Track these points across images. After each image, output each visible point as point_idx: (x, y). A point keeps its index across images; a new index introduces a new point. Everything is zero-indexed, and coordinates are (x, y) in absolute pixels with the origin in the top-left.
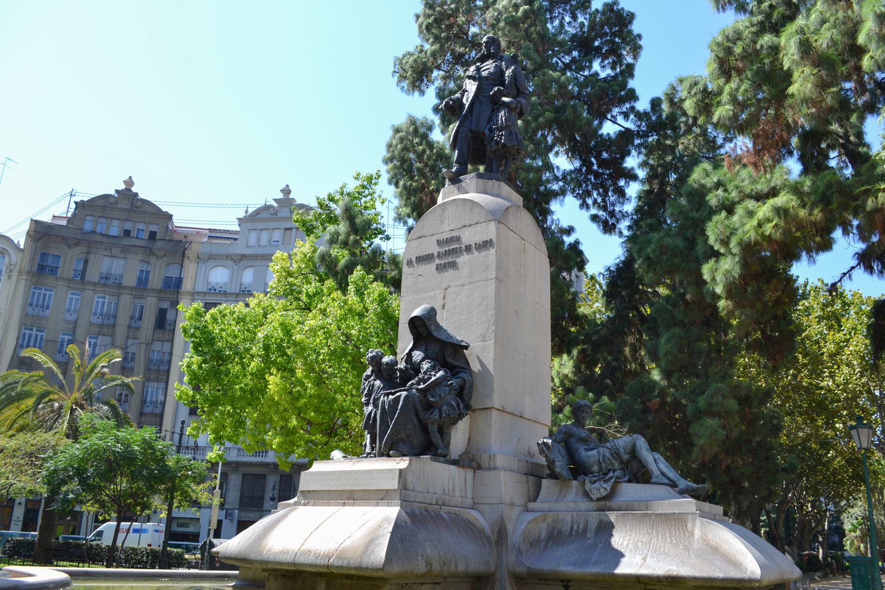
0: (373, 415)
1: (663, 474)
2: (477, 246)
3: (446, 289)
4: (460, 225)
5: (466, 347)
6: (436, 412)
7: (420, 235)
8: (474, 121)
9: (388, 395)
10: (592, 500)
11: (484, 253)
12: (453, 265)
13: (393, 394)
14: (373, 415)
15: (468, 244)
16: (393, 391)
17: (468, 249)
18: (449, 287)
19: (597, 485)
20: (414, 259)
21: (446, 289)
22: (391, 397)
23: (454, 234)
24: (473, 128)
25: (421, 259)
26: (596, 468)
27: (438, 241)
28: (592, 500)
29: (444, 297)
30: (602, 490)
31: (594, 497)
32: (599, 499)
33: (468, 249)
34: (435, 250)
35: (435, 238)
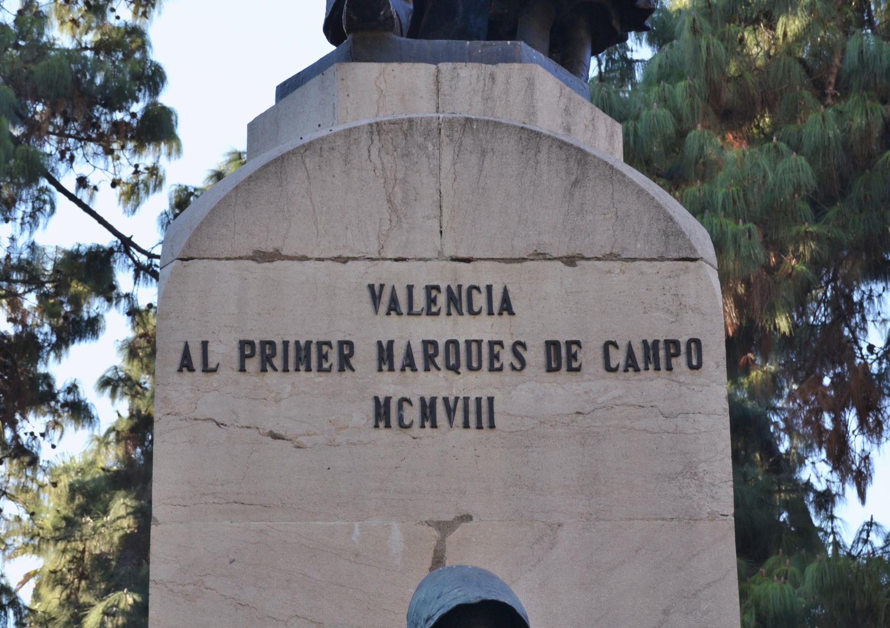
2: (618, 358)
4: (521, 248)
15: (562, 338)
18: (468, 518)
23: (467, 276)
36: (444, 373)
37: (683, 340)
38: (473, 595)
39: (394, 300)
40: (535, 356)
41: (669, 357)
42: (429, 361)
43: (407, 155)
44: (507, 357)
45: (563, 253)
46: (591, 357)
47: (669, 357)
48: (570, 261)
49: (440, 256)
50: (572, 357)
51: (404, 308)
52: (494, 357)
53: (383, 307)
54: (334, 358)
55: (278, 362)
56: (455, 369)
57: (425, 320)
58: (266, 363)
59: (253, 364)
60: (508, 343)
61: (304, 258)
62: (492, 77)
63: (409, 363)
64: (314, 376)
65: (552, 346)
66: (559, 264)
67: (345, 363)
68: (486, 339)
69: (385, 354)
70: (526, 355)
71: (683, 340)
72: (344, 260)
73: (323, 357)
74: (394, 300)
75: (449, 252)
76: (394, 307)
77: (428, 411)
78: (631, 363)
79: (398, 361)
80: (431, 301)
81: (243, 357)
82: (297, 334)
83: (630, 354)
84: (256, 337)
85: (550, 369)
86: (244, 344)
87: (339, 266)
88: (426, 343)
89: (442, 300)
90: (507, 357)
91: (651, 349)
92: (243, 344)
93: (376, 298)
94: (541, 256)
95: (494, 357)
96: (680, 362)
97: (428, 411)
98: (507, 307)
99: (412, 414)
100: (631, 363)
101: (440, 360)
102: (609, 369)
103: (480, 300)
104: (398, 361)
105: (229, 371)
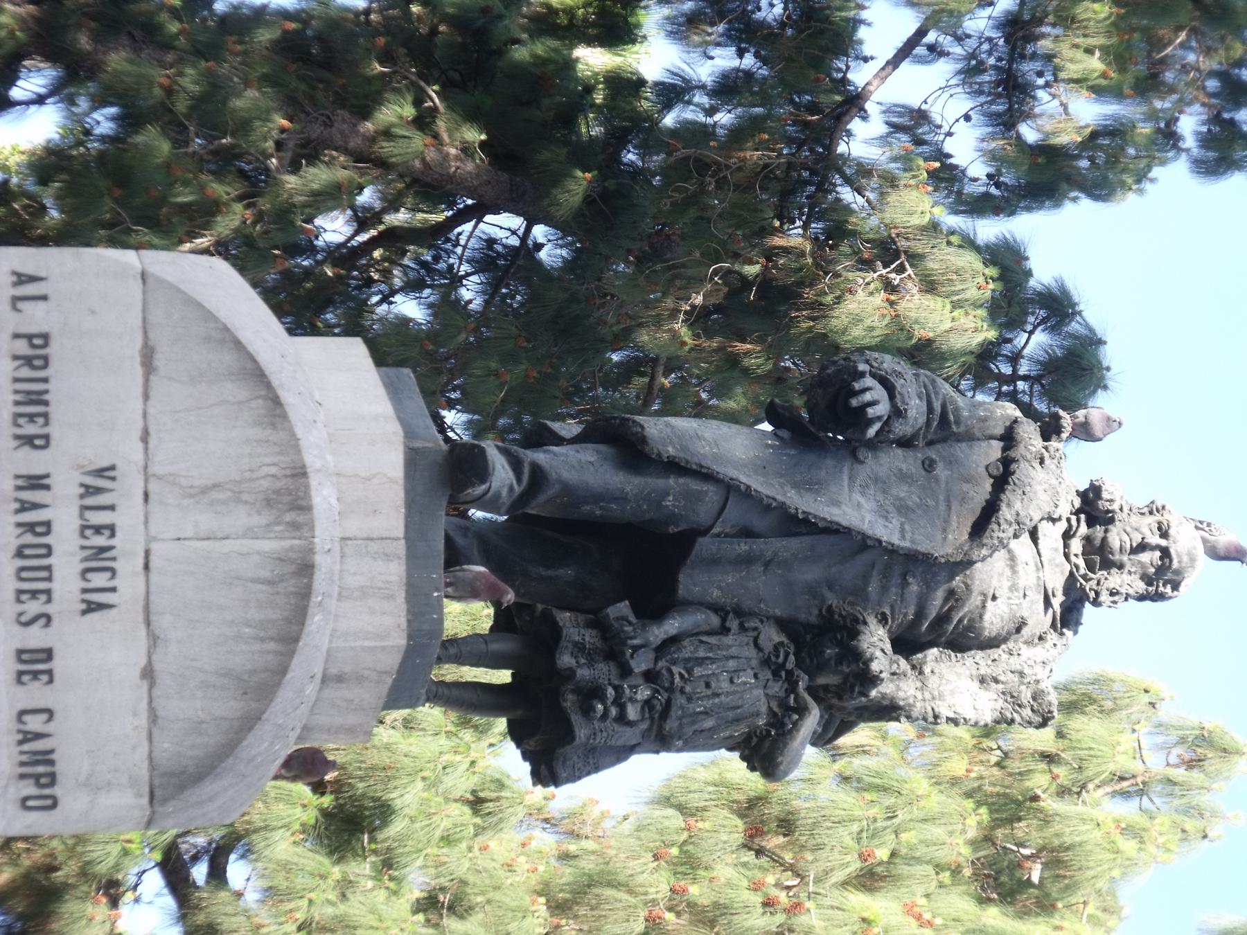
2: (35, 723)
4: (163, 622)
7: (160, 361)
8: (743, 547)
15: (56, 664)
20: (36, 317)
24: (704, 545)
27: (104, 472)
36: (14, 543)
37: (57, 791)
39: (99, 491)
40: (36, 637)
41: (37, 777)
42: (30, 527)
43: (268, 503)
44: (33, 607)
45: (157, 666)
46: (36, 695)
47: (37, 777)
48: (148, 674)
49: (150, 539)
50: (35, 675)
51: (89, 501)
52: (34, 594)
53: (90, 481)
54: (30, 429)
55: (26, 372)
56: (19, 554)
57: (77, 523)
58: (28, 361)
59: (22, 347)
60: (49, 609)
61: (146, 397)
62: (390, 597)
63: (25, 507)
64: (8, 410)
65: (48, 654)
66: (143, 661)
67: (28, 441)
68: (55, 586)
69: (37, 482)
70: (35, 629)
71: (57, 791)
72: (145, 437)
73: (31, 417)
74: (99, 491)
75: (156, 547)
76: (89, 491)
78: (29, 737)
79: (28, 496)
80: (98, 530)
81: (30, 337)
83: (38, 736)
84: (53, 350)
85: (20, 652)
86: (45, 337)
87: (137, 433)
88: (48, 524)
89: (100, 541)
90: (33, 607)
91: (45, 758)
92: (45, 337)
93: (100, 472)
95: (34, 594)
96: (29, 789)
98: (92, 608)
100: (29, 737)
101: (29, 539)
102: (23, 713)
103: (99, 580)
104: (28, 496)
105: (14, 322)
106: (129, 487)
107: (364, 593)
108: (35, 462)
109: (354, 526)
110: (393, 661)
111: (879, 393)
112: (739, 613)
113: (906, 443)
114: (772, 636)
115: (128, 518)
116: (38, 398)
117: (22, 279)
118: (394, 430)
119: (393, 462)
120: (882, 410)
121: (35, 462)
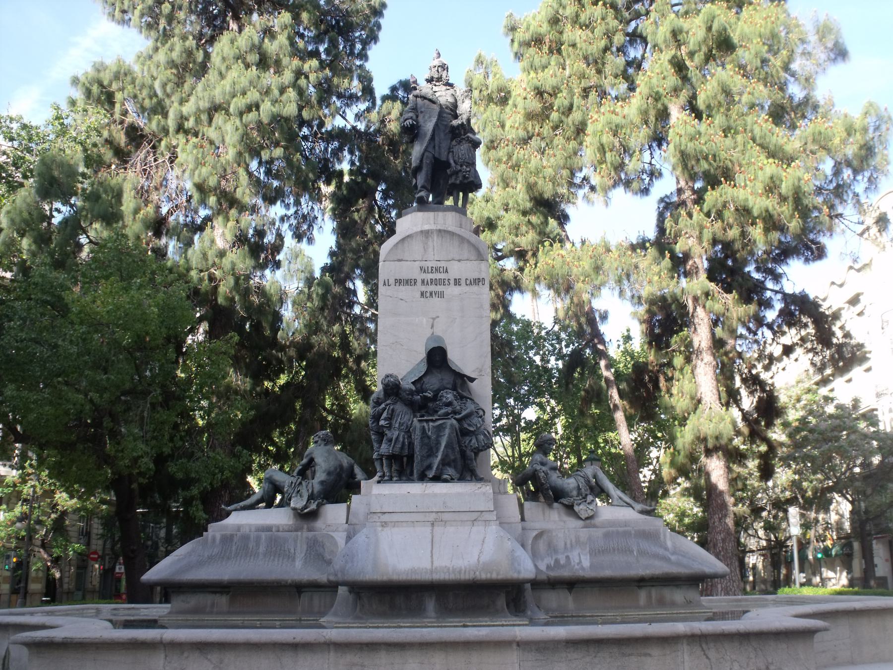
0: (401, 439)
1: (620, 498)
2: (468, 282)
3: (434, 319)
5: (472, 380)
6: (474, 441)
8: (437, 148)
9: (427, 421)
10: (581, 519)
11: (475, 288)
12: (441, 295)
13: (432, 421)
14: (401, 439)
16: (434, 418)
17: (457, 282)
19: (581, 507)
20: (392, 281)
21: (434, 319)
22: (431, 424)
23: (439, 264)
24: (437, 155)
25: (399, 282)
26: (575, 493)
28: (581, 519)
29: (432, 327)
30: (589, 511)
31: (583, 517)
32: (587, 518)
33: (457, 282)
34: (420, 276)
35: (417, 264)
38: (436, 345)
40: (452, 282)
44: (447, 282)
46: (463, 282)
48: (459, 261)
63: (428, 284)
69: (423, 281)
77: (431, 294)
78: (471, 283)
82: (406, 277)
90: (447, 282)
94: (453, 260)
97: (431, 294)
98: (447, 271)
99: (428, 294)
100: (471, 283)
105: (393, 286)
106: (424, 264)
107: (444, 220)
108: (419, 282)
109: (432, 222)
110: (458, 215)
111: (407, 122)
112: (449, 149)
113: (417, 117)
114: (454, 143)
115: (430, 264)
116: (407, 281)
117: (385, 284)
118: (414, 214)
119: (420, 214)
120: (410, 121)
121: (419, 282)
